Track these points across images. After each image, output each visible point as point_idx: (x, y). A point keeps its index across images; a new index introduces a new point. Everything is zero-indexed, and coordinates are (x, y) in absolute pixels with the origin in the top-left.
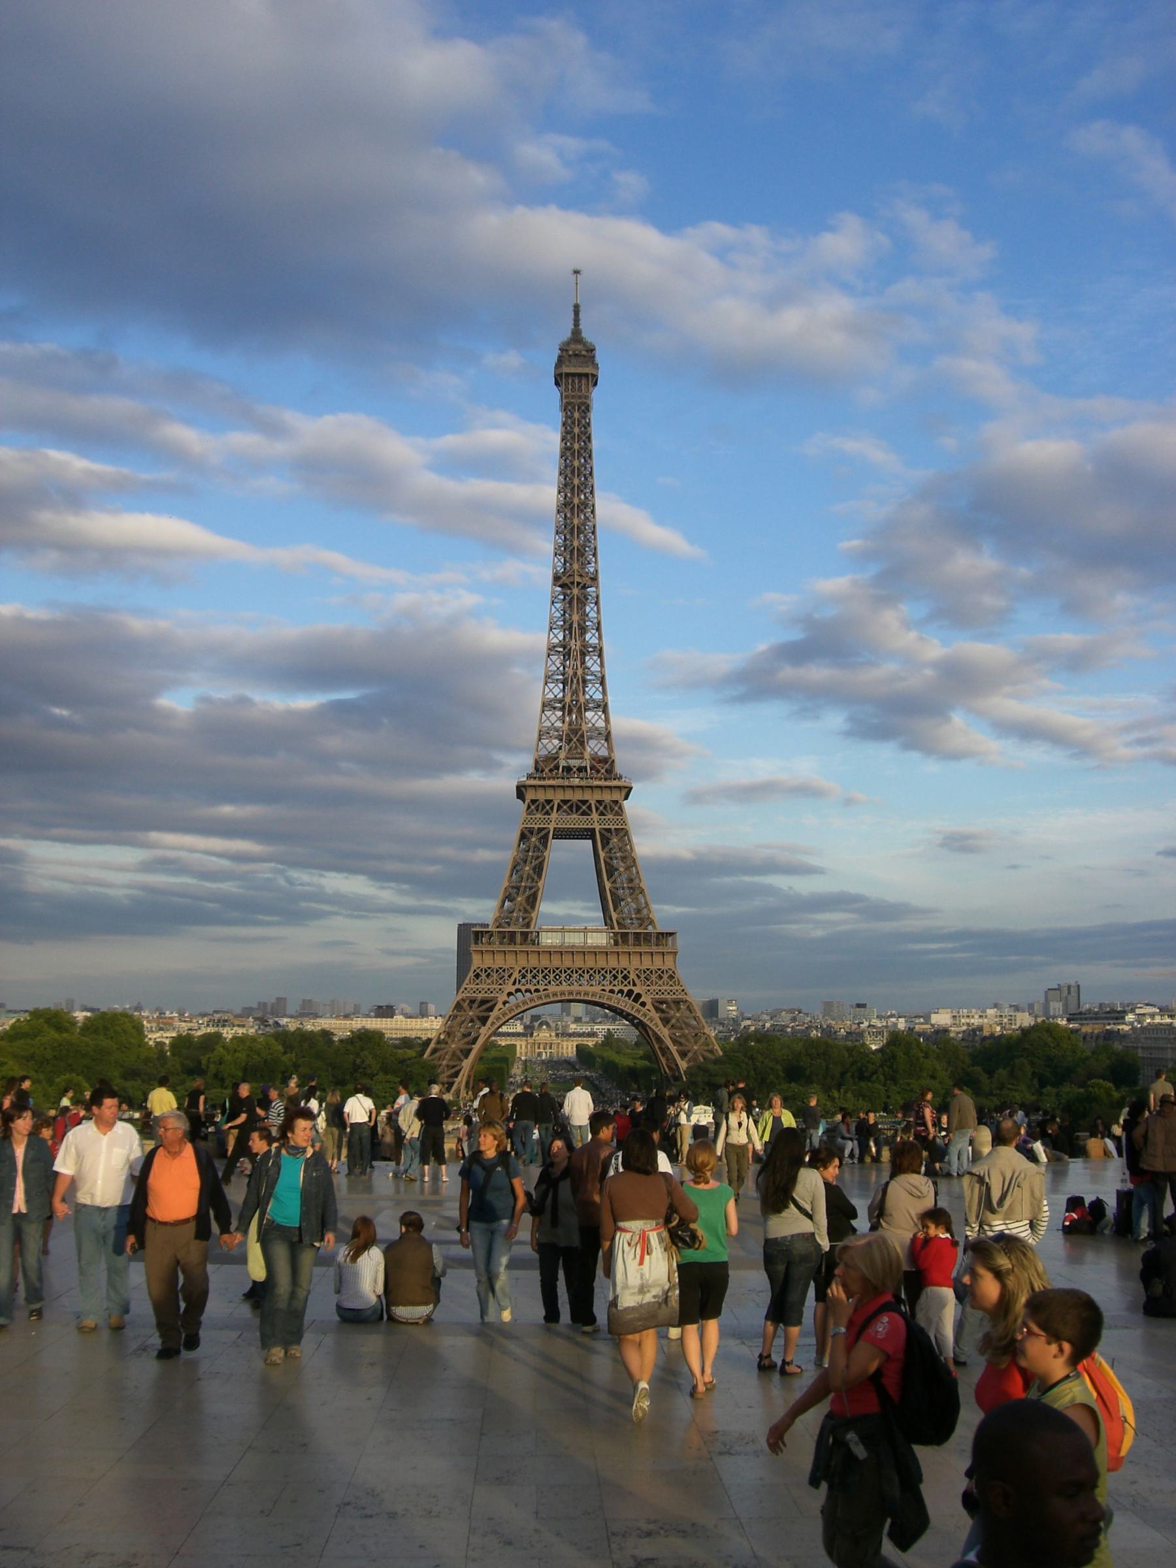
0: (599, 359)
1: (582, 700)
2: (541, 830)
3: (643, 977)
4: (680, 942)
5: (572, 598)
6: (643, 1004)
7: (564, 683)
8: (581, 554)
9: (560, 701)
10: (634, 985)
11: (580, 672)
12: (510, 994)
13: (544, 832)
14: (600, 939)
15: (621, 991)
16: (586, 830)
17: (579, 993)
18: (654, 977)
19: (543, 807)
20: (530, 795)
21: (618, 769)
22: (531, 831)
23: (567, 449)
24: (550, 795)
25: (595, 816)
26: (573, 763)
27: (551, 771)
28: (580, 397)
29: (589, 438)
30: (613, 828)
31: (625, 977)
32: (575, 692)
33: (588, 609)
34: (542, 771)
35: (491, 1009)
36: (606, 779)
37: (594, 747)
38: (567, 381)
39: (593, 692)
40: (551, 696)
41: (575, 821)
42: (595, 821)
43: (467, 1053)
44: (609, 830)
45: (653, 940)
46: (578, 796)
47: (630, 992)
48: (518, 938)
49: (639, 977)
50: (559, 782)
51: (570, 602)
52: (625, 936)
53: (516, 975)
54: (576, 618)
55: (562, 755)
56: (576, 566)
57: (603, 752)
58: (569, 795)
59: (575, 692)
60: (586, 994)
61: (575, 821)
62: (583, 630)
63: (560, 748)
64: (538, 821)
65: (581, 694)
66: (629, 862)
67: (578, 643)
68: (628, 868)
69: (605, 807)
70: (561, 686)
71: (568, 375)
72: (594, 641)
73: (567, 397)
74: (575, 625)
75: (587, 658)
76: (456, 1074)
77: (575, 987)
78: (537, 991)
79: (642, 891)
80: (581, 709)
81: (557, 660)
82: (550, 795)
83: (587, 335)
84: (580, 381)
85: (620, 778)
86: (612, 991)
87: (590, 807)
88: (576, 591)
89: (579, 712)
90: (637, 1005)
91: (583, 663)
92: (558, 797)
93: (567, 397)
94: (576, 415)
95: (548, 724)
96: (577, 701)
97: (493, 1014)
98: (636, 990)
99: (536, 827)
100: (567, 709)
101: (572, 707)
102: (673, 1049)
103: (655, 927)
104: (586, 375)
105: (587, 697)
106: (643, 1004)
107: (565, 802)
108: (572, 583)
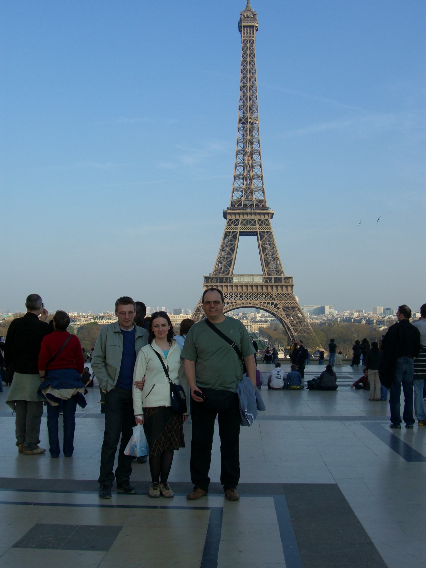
1: (252, 174)
2: (233, 232)
3: (278, 296)
4: (295, 282)
5: (247, 129)
6: (278, 308)
7: (243, 167)
8: (250, 109)
9: (243, 175)
10: (274, 300)
11: (250, 162)
13: (234, 234)
14: (260, 280)
16: (254, 232)
17: (250, 304)
18: (283, 296)
19: (235, 222)
20: (229, 217)
21: (268, 205)
22: (229, 232)
23: (244, 61)
24: (237, 217)
26: (247, 203)
27: (238, 206)
28: (250, 37)
29: (254, 55)
30: (265, 231)
31: (271, 297)
32: (249, 171)
33: (254, 134)
34: (234, 206)
36: (262, 210)
37: (257, 196)
38: (244, 30)
39: (256, 171)
40: (238, 173)
41: (249, 228)
42: (258, 228)
44: (263, 232)
45: (283, 281)
46: (250, 217)
47: (272, 303)
48: (224, 280)
49: (276, 297)
50: (242, 211)
51: (246, 130)
52: (270, 279)
54: (248, 138)
55: (243, 199)
56: (248, 114)
57: (262, 198)
59: (249, 171)
60: (254, 304)
62: (252, 143)
63: (242, 196)
64: (233, 228)
65: (251, 172)
66: (272, 246)
67: (250, 149)
68: (273, 248)
69: (262, 222)
70: (242, 168)
71: (244, 27)
72: (257, 148)
73: (244, 37)
74: (248, 141)
75: (254, 156)
77: (248, 301)
78: (232, 303)
79: (278, 259)
81: (241, 156)
82: (237, 217)
84: (250, 30)
85: (268, 208)
86: (265, 303)
87: (255, 222)
88: (248, 126)
89: (250, 179)
90: (276, 309)
91: (252, 158)
92: (241, 218)
93: (244, 37)
94: (248, 45)
95: (236, 185)
96: (250, 175)
98: (275, 302)
99: (231, 231)
101: (248, 179)
102: (291, 328)
103: (284, 275)
104: (252, 27)
105: (254, 173)
106: (278, 308)
107: (244, 220)
108: (247, 122)
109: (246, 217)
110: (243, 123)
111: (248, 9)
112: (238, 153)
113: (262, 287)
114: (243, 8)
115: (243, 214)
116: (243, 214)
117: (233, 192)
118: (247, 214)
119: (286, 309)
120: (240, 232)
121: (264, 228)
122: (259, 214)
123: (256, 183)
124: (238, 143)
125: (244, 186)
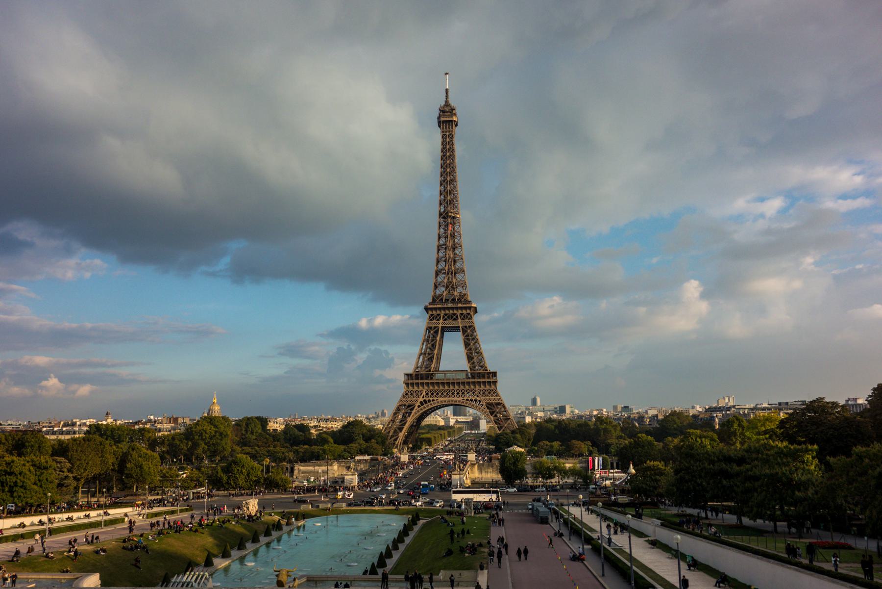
4: (499, 378)
7: (445, 261)
12: (421, 403)
15: (471, 400)
20: (430, 312)
21: (469, 299)
22: (431, 328)
24: (438, 312)
25: (459, 320)
35: (412, 409)
39: (458, 264)
41: (450, 323)
42: (460, 323)
43: (401, 429)
53: (424, 393)
58: (447, 312)
61: (450, 323)
76: (396, 440)
81: (442, 251)
82: (438, 312)
83: (452, 103)
85: (470, 302)
88: (449, 220)
95: (439, 280)
98: (479, 399)
107: (446, 315)
109: (447, 312)
110: (444, 218)
111: (447, 104)
112: (439, 248)
113: (463, 383)
114: (443, 103)
115: (444, 309)
116: (444, 309)
118: (448, 309)
121: (467, 323)
122: (461, 308)
123: (459, 276)
125: (446, 281)
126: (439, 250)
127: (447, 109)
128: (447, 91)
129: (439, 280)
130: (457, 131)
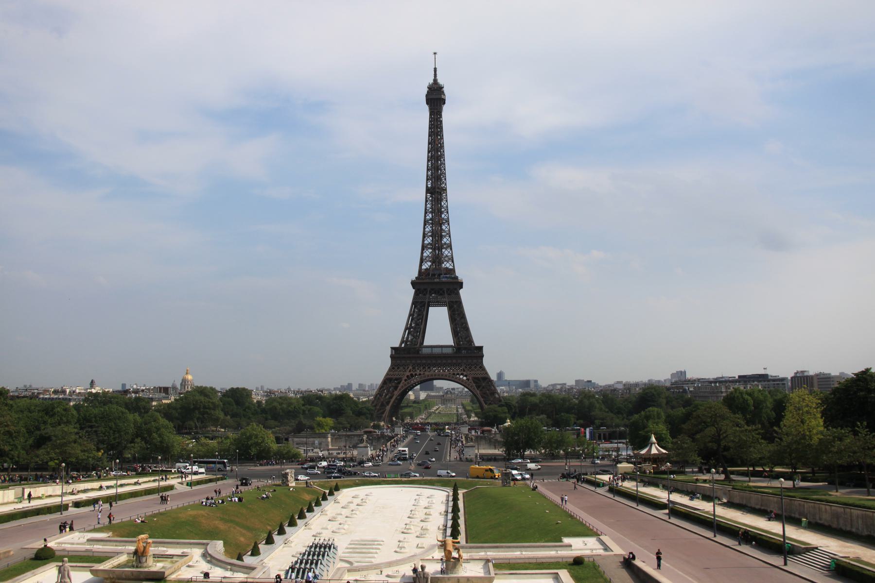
0: (445, 90)
14: (450, 351)
25: (446, 295)
35: (399, 383)
37: (447, 265)
43: (388, 403)
53: (411, 368)
57: (451, 267)
76: (383, 413)
80: (440, 248)
83: (440, 81)
85: (457, 278)
97: (401, 384)
100: (434, 249)
102: (482, 400)
107: (432, 289)
114: (431, 81)
117: (422, 261)
119: (477, 380)
120: (429, 302)
123: (446, 252)
124: (426, 213)
126: (425, 225)
127: (436, 87)
128: (435, 70)
129: (425, 254)
130: (446, 109)
